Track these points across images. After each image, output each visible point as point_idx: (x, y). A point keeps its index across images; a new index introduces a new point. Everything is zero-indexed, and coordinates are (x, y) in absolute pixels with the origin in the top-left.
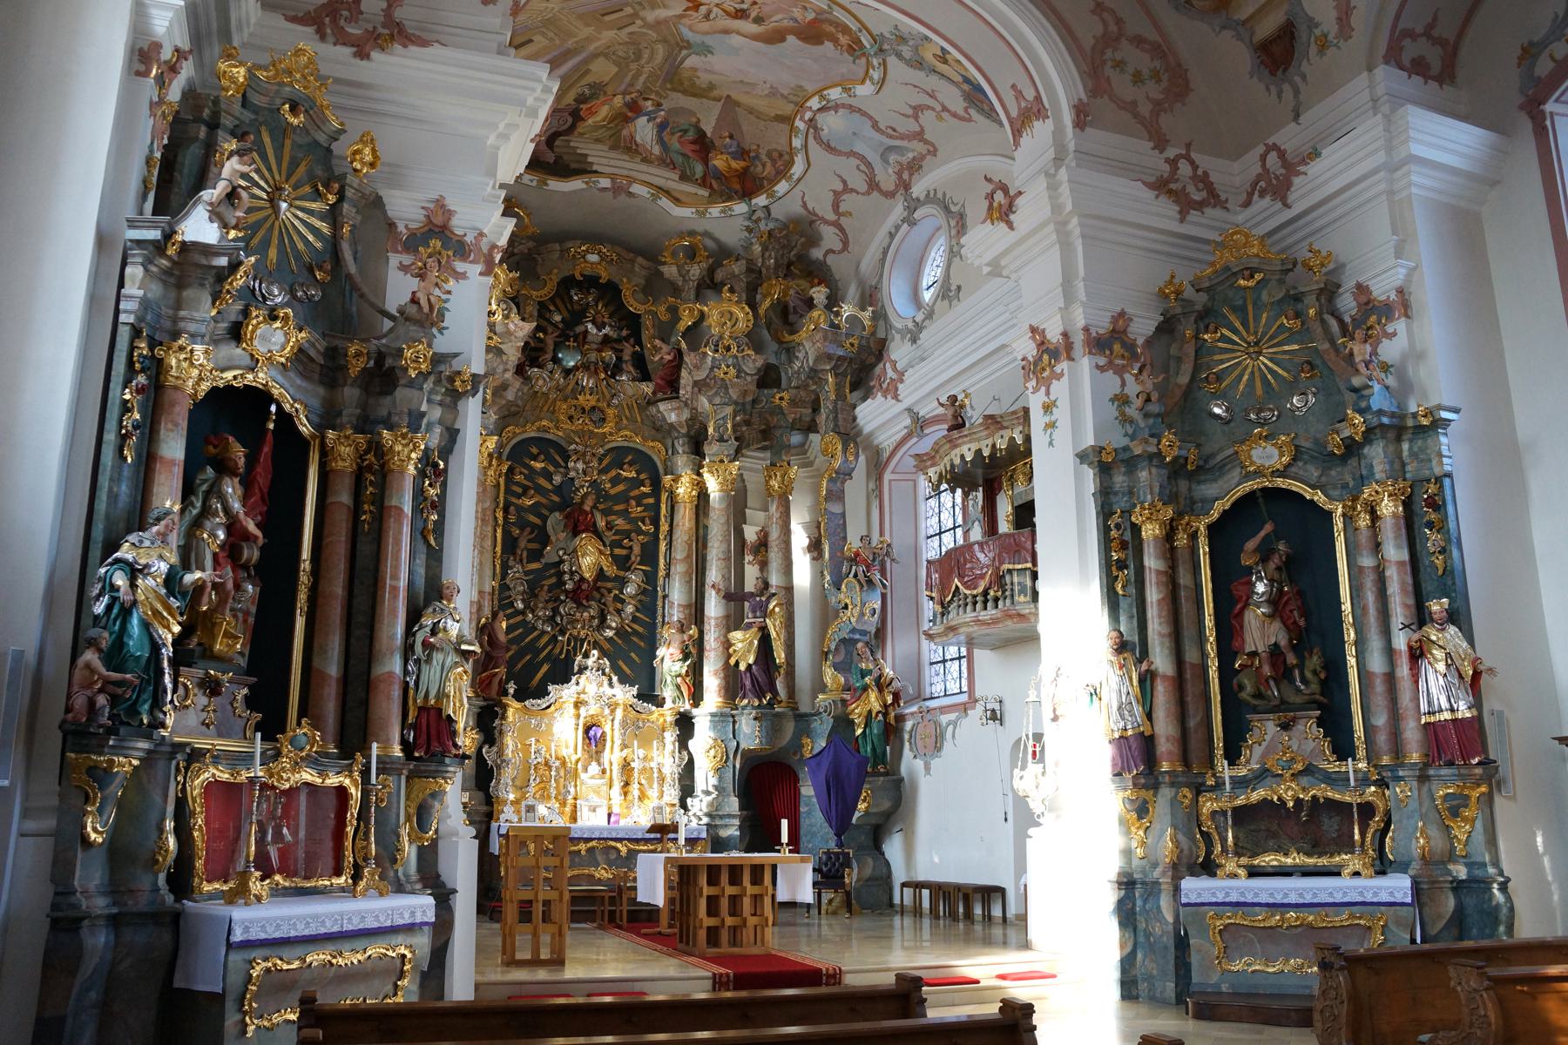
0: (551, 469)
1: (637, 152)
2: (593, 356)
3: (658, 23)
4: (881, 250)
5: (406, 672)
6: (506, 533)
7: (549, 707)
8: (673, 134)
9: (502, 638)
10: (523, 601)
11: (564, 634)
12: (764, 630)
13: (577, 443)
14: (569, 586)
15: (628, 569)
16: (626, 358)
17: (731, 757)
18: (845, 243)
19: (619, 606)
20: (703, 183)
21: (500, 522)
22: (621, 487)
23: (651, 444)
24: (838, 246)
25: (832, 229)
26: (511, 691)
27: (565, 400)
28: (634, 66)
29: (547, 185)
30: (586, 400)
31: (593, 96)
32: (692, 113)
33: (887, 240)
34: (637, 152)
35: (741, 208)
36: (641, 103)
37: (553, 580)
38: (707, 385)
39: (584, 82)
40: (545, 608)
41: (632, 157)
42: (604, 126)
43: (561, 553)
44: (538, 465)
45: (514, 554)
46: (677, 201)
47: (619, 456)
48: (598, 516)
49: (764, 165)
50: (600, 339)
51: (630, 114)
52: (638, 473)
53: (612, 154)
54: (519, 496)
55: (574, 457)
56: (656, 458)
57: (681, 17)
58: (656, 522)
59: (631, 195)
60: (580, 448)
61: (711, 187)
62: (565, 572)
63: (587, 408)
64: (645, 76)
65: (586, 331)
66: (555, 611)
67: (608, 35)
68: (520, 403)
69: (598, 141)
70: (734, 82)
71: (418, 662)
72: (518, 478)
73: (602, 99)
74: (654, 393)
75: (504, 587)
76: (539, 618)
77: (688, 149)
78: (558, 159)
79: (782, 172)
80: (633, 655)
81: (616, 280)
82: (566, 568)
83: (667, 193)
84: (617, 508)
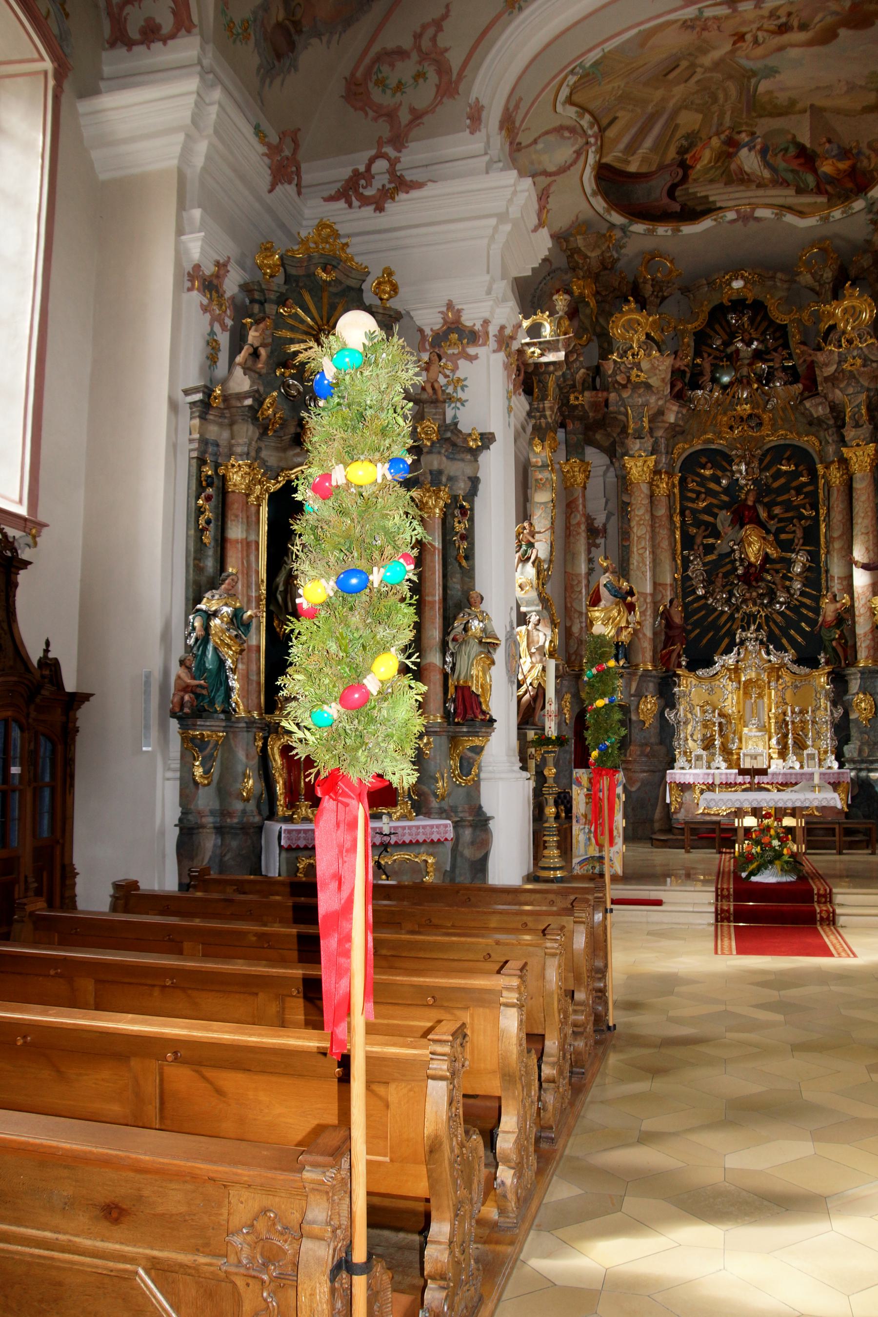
0: (719, 473)
1: (750, 181)
2: (745, 371)
3: (717, 65)
5: (445, 662)
6: (684, 534)
7: (717, 674)
8: (776, 155)
9: (677, 619)
10: (704, 587)
11: (738, 612)
15: (793, 551)
19: (787, 583)
22: (782, 481)
26: (684, 663)
27: (725, 413)
28: (715, 108)
29: (680, 231)
31: (692, 145)
34: (750, 181)
35: (859, 205)
36: (736, 137)
37: (729, 567)
38: (837, 379)
39: (678, 135)
40: (722, 592)
42: (712, 167)
43: (731, 543)
44: (708, 473)
46: (801, 214)
47: (779, 453)
49: (869, 158)
50: (750, 354)
51: (731, 150)
52: (796, 466)
53: (730, 189)
54: (693, 501)
56: (811, 450)
57: (733, 52)
58: (815, 506)
59: (758, 220)
60: (740, 452)
61: (827, 192)
62: (736, 560)
63: (745, 417)
64: (729, 113)
65: (738, 350)
66: (731, 594)
67: (679, 91)
68: (681, 423)
69: (712, 181)
71: (452, 655)
73: (700, 145)
74: (801, 394)
75: (686, 579)
76: (718, 601)
77: (795, 164)
78: (683, 207)
81: (761, 298)
82: (737, 555)
83: (790, 209)
84: (779, 499)
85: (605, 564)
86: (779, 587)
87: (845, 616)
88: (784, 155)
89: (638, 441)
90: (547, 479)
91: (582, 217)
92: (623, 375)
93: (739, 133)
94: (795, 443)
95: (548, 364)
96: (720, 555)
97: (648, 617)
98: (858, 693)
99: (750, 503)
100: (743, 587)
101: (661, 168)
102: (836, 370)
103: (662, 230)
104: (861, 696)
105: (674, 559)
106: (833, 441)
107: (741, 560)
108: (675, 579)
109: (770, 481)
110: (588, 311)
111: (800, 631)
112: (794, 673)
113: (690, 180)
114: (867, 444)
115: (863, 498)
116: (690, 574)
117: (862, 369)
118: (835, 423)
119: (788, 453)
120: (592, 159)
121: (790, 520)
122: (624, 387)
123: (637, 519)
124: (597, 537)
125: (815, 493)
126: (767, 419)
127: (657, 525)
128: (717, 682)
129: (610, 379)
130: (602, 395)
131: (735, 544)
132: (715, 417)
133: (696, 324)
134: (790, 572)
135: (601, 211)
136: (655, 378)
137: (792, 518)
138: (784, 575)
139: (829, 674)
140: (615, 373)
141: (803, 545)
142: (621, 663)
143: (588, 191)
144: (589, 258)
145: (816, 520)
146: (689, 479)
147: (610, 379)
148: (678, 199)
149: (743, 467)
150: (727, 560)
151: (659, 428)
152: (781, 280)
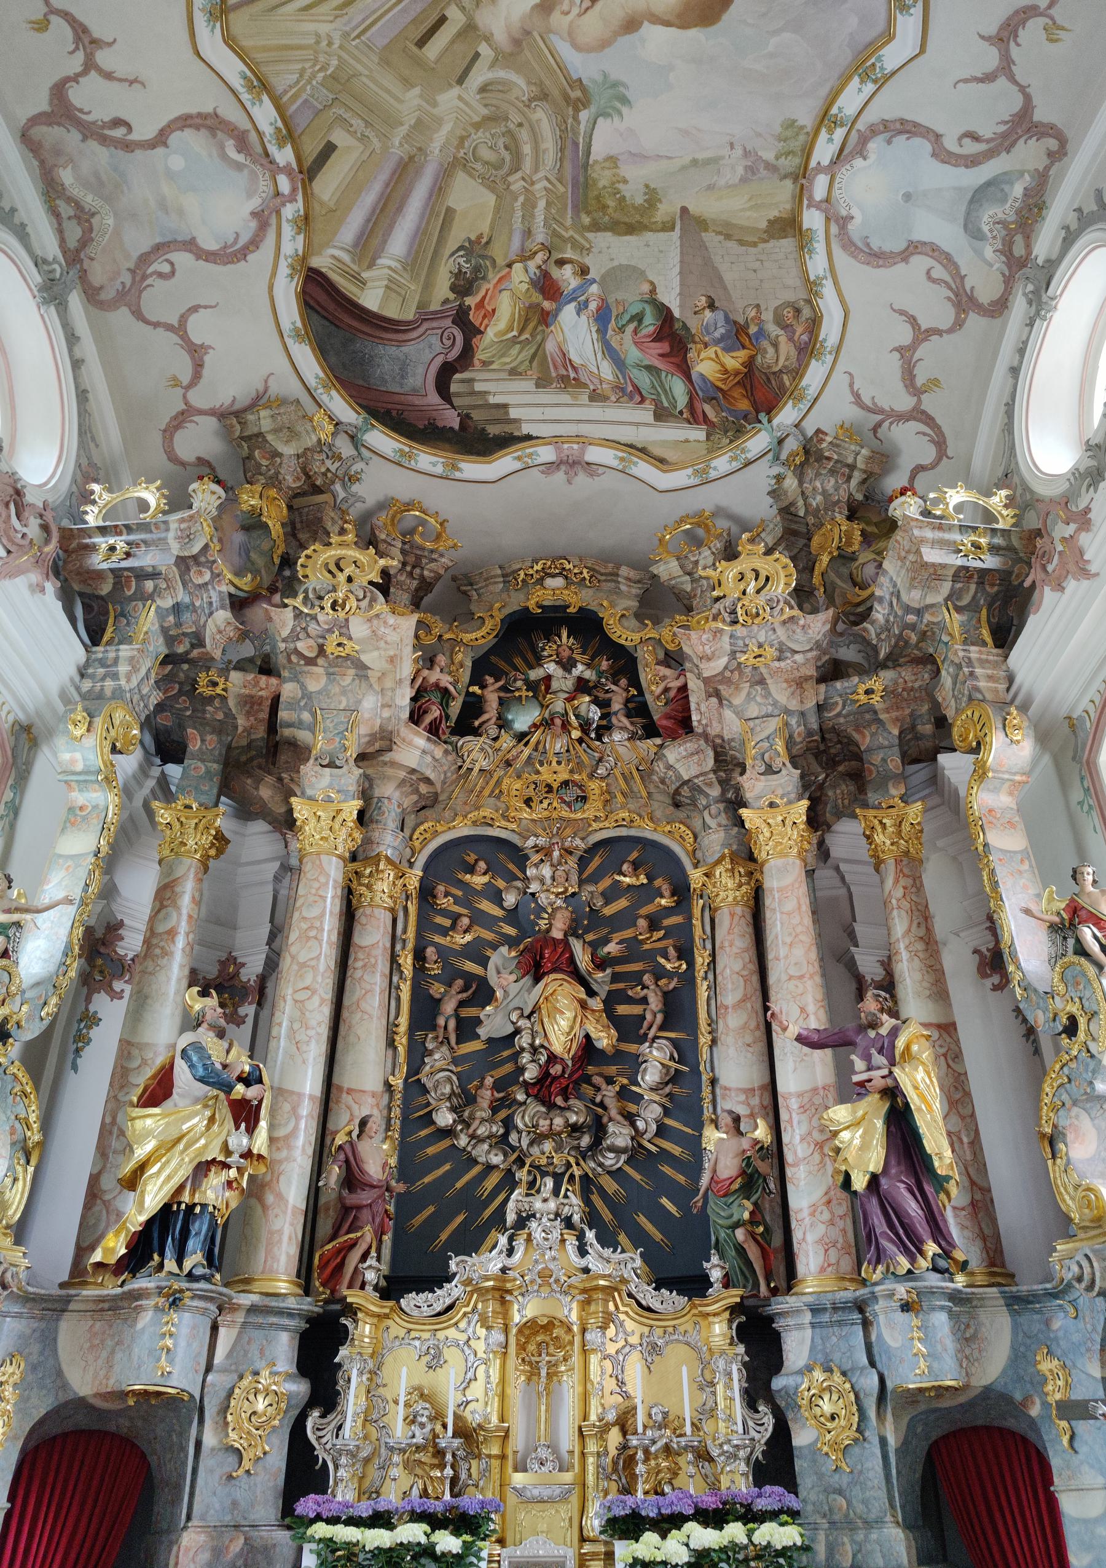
0: (501, 883)
1: (579, 384)
2: (559, 706)
4: (1003, 409)
7: (450, 1307)
8: (622, 329)
10: (453, 1109)
12: (892, 1093)
13: (537, 836)
14: (532, 1073)
15: (642, 1039)
16: (617, 705)
17: (872, 1413)
18: (940, 444)
19: (632, 1108)
20: (694, 416)
21: (408, 971)
22: (622, 903)
23: (668, 828)
24: (928, 454)
25: (914, 426)
26: (371, 1276)
29: (459, 470)
30: (554, 773)
32: (639, 274)
33: (1011, 381)
34: (579, 384)
35: (758, 442)
36: (555, 273)
37: (508, 1068)
39: (452, 245)
40: (491, 1120)
41: (574, 396)
42: (514, 341)
43: (514, 1018)
44: (478, 880)
45: (434, 1027)
46: (661, 462)
48: (577, 946)
51: (547, 305)
52: (651, 878)
54: (444, 932)
55: (535, 858)
58: (685, 953)
60: (542, 841)
62: (523, 1049)
63: (555, 785)
64: (542, 204)
66: (508, 1124)
69: (514, 372)
70: (684, 168)
72: (444, 902)
73: (493, 277)
75: (415, 1087)
78: (465, 418)
79: (808, 350)
80: (664, 1201)
81: (593, 607)
82: (524, 1040)
85: (197, 1007)
86: (613, 1113)
87: (763, 1167)
88: (635, 332)
89: (327, 770)
90: (95, 807)
91: (274, 389)
92: (311, 642)
93: (561, 263)
94: (648, 835)
95: (141, 575)
96: (490, 1040)
97: (298, 1154)
98: (809, 1369)
99: (557, 934)
100: (535, 1108)
101: (425, 317)
102: (726, 668)
103: (428, 460)
104: (818, 1375)
105: (391, 1044)
106: (720, 825)
107: (534, 1050)
108: (388, 1086)
109: (599, 903)
110: (266, 545)
111: (660, 1217)
112: (649, 1309)
113: (476, 362)
114: (790, 802)
115: (790, 905)
116: (424, 1080)
117: (776, 664)
118: (724, 792)
119: (634, 855)
120: (292, 244)
121: (636, 978)
122: (311, 662)
123: (304, 926)
124: (243, 1000)
125: (688, 925)
126: (597, 792)
127: (359, 964)
128: (452, 1333)
129: (282, 646)
130: (266, 685)
131: (522, 1016)
132: (499, 783)
133: (479, 634)
134: (638, 1085)
135: (312, 382)
136: (376, 654)
137: (642, 973)
138: (623, 1087)
139: (735, 1310)
140: (294, 637)
141: (662, 1028)
142: (194, 1259)
143: (286, 325)
144: (280, 455)
145: (688, 979)
146: (441, 889)
147: (282, 646)
148: (457, 401)
149: (546, 871)
150: (506, 1054)
151: (384, 778)
152: (628, 579)
